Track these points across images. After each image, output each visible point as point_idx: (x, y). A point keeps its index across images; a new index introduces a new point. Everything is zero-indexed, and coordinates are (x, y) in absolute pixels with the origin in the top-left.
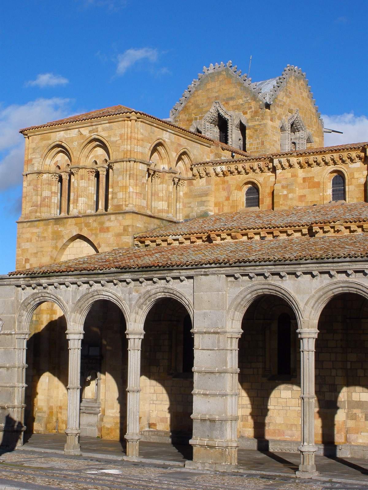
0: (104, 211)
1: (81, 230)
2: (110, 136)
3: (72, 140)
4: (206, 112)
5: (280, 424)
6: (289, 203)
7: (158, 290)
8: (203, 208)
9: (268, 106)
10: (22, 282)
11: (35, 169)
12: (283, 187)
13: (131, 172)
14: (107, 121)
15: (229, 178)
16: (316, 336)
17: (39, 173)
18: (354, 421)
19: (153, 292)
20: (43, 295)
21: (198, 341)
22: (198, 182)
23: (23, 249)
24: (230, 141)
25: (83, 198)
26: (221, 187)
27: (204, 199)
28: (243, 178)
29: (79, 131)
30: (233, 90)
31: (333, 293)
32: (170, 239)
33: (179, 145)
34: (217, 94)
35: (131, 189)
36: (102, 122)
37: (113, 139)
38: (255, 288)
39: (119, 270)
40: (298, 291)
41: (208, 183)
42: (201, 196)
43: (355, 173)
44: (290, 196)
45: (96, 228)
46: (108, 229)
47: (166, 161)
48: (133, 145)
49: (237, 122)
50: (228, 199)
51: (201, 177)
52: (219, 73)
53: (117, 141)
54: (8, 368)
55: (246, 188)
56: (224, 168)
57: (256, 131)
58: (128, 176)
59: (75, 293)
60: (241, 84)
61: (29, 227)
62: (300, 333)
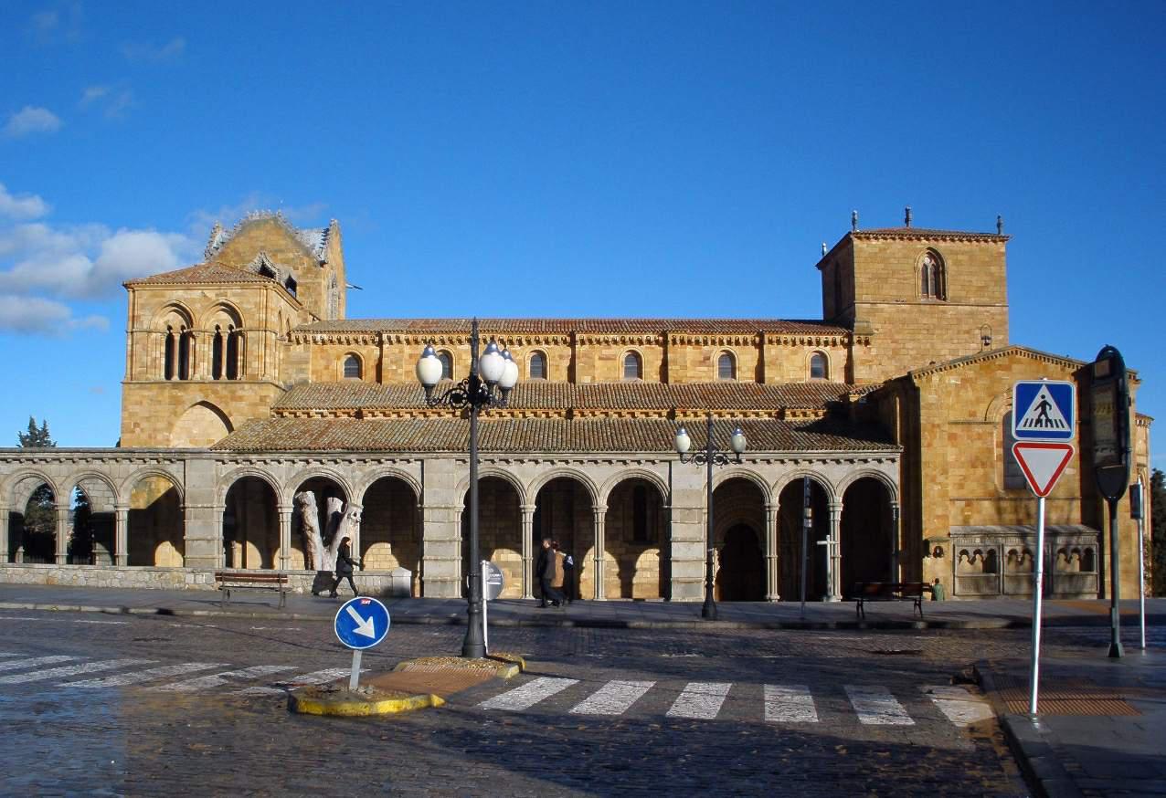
0: (211, 377)
1: (207, 396)
3: (193, 301)
4: (249, 261)
6: (398, 377)
8: (302, 376)
9: (322, 264)
10: (226, 457)
11: (145, 327)
12: (392, 362)
15: (328, 346)
17: (149, 332)
21: (426, 514)
22: (295, 349)
23: (130, 413)
27: (304, 366)
28: (345, 348)
30: (282, 242)
32: (312, 412)
34: (263, 244)
39: (346, 451)
40: (523, 474)
41: (306, 350)
44: (399, 371)
45: (226, 396)
46: (241, 399)
49: (285, 277)
50: (327, 368)
51: (298, 343)
52: (266, 222)
54: (209, 541)
55: (344, 359)
56: (325, 337)
57: (309, 288)
59: (290, 470)
61: (139, 388)
62: (524, 509)
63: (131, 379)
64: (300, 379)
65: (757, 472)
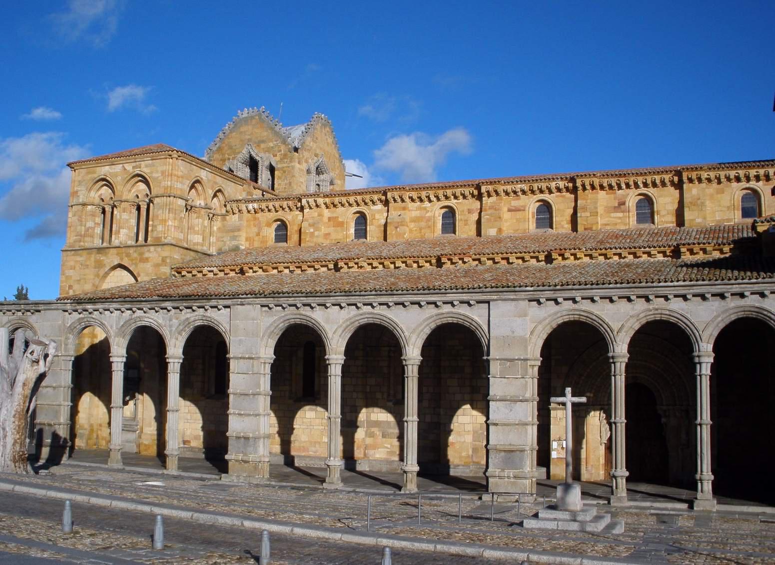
0: (144, 242)
1: (122, 259)
2: (152, 173)
3: (116, 175)
4: (239, 153)
5: (305, 442)
6: (315, 240)
7: (197, 318)
8: (234, 243)
9: (296, 150)
10: (68, 307)
11: (81, 201)
12: (310, 225)
13: (171, 207)
14: (150, 159)
16: (343, 362)
18: (372, 438)
19: (192, 319)
20: (89, 320)
21: (233, 365)
22: (231, 218)
24: (259, 181)
25: (124, 230)
26: (252, 223)
27: (236, 234)
28: (273, 215)
29: (123, 167)
30: (265, 134)
31: (359, 323)
32: (205, 270)
33: (216, 183)
34: (249, 137)
35: (170, 223)
36: (145, 159)
37: (155, 175)
38: (288, 317)
39: (161, 298)
40: (327, 321)
41: (240, 219)
42: (233, 231)
44: (316, 233)
45: (136, 259)
46: (147, 260)
47: (202, 197)
48: (173, 182)
49: (267, 163)
50: (258, 234)
51: (234, 214)
52: (252, 118)
53: (158, 177)
54: (54, 388)
55: (275, 225)
56: (256, 205)
57: (285, 172)
58: (167, 210)
59: (119, 319)
60: (272, 129)
61: (73, 255)
62: (328, 359)
64: (233, 245)
65: (596, 312)
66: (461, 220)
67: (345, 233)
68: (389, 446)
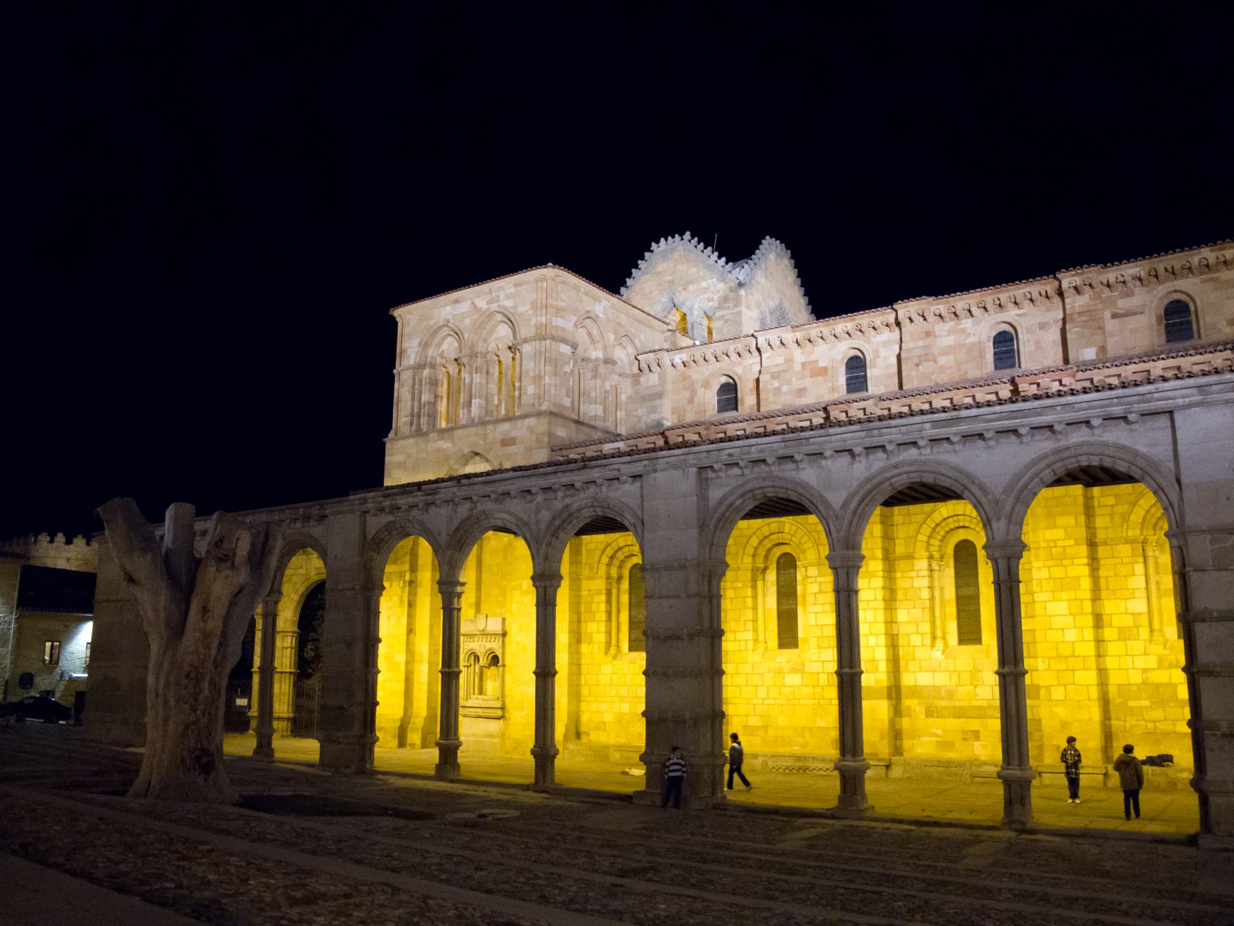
2: (515, 307)
3: (463, 316)
8: (654, 417)
13: (547, 355)
25: (477, 400)
27: (656, 402)
29: (473, 303)
34: (670, 278)
35: (547, 380)
37: (521, 309)
38: (749, 487)
43: (880, 350)
47: (600, 346)
48: (549, 316)
50: (691, 401)
53: (526, 312)
58: (543, 361)
63: (396, 435)
64: (653, 421)
66: (1028, 341)
67: (830, 384)
68: (939, 732)
